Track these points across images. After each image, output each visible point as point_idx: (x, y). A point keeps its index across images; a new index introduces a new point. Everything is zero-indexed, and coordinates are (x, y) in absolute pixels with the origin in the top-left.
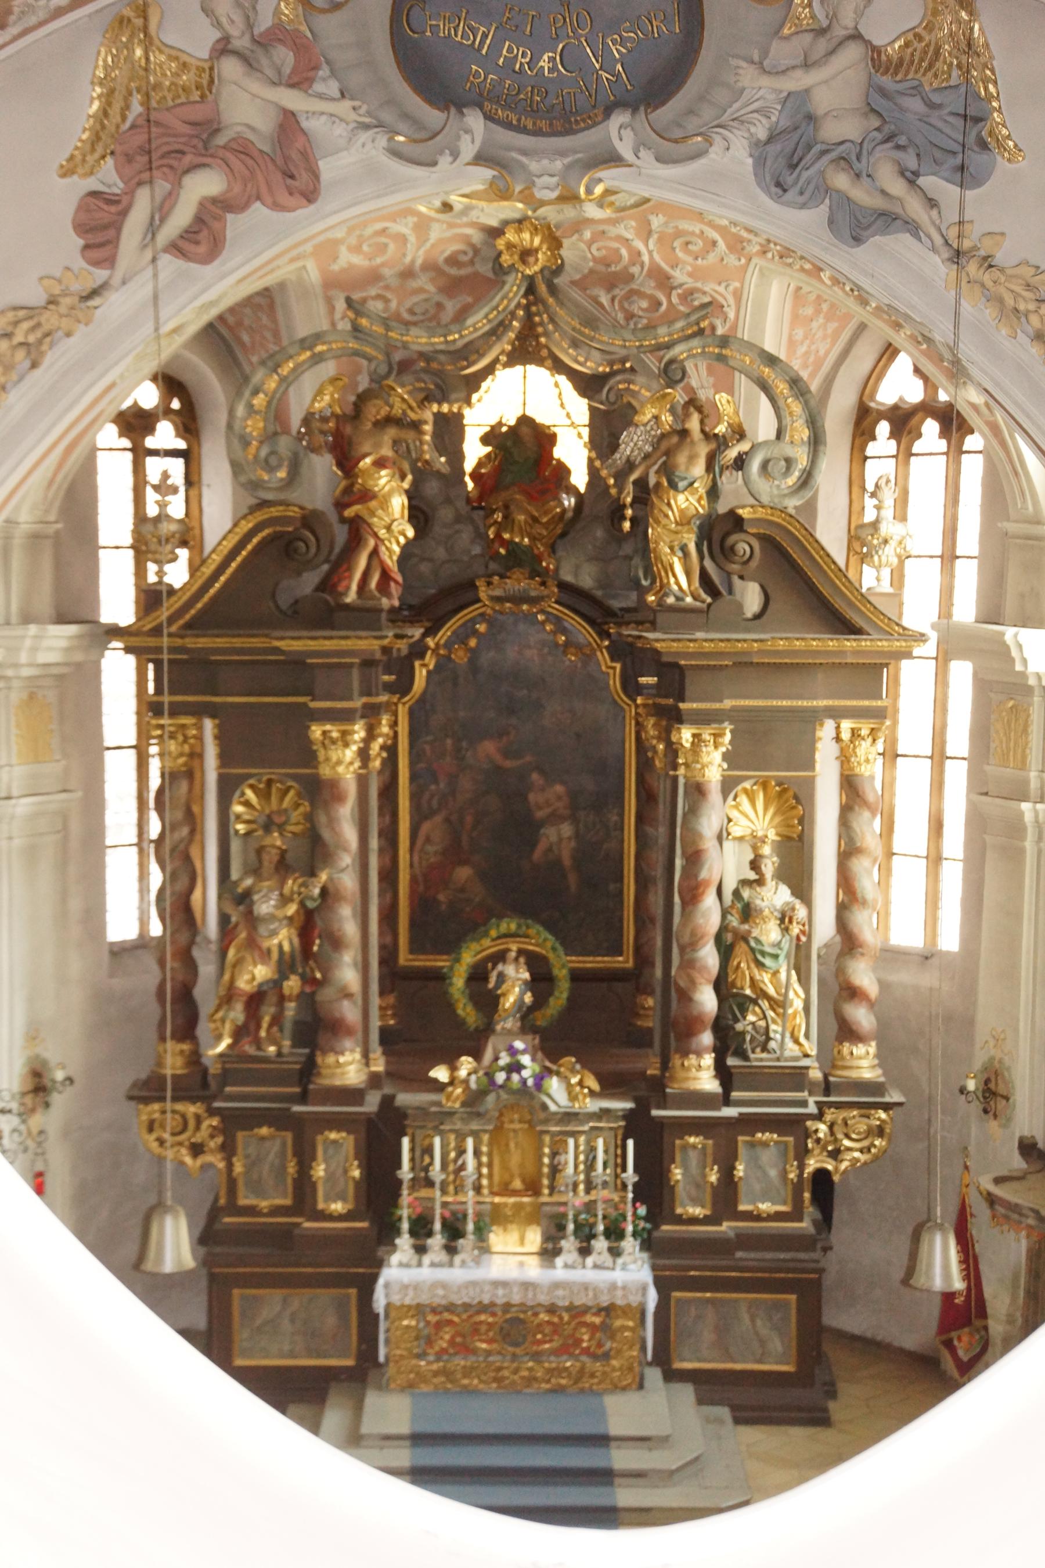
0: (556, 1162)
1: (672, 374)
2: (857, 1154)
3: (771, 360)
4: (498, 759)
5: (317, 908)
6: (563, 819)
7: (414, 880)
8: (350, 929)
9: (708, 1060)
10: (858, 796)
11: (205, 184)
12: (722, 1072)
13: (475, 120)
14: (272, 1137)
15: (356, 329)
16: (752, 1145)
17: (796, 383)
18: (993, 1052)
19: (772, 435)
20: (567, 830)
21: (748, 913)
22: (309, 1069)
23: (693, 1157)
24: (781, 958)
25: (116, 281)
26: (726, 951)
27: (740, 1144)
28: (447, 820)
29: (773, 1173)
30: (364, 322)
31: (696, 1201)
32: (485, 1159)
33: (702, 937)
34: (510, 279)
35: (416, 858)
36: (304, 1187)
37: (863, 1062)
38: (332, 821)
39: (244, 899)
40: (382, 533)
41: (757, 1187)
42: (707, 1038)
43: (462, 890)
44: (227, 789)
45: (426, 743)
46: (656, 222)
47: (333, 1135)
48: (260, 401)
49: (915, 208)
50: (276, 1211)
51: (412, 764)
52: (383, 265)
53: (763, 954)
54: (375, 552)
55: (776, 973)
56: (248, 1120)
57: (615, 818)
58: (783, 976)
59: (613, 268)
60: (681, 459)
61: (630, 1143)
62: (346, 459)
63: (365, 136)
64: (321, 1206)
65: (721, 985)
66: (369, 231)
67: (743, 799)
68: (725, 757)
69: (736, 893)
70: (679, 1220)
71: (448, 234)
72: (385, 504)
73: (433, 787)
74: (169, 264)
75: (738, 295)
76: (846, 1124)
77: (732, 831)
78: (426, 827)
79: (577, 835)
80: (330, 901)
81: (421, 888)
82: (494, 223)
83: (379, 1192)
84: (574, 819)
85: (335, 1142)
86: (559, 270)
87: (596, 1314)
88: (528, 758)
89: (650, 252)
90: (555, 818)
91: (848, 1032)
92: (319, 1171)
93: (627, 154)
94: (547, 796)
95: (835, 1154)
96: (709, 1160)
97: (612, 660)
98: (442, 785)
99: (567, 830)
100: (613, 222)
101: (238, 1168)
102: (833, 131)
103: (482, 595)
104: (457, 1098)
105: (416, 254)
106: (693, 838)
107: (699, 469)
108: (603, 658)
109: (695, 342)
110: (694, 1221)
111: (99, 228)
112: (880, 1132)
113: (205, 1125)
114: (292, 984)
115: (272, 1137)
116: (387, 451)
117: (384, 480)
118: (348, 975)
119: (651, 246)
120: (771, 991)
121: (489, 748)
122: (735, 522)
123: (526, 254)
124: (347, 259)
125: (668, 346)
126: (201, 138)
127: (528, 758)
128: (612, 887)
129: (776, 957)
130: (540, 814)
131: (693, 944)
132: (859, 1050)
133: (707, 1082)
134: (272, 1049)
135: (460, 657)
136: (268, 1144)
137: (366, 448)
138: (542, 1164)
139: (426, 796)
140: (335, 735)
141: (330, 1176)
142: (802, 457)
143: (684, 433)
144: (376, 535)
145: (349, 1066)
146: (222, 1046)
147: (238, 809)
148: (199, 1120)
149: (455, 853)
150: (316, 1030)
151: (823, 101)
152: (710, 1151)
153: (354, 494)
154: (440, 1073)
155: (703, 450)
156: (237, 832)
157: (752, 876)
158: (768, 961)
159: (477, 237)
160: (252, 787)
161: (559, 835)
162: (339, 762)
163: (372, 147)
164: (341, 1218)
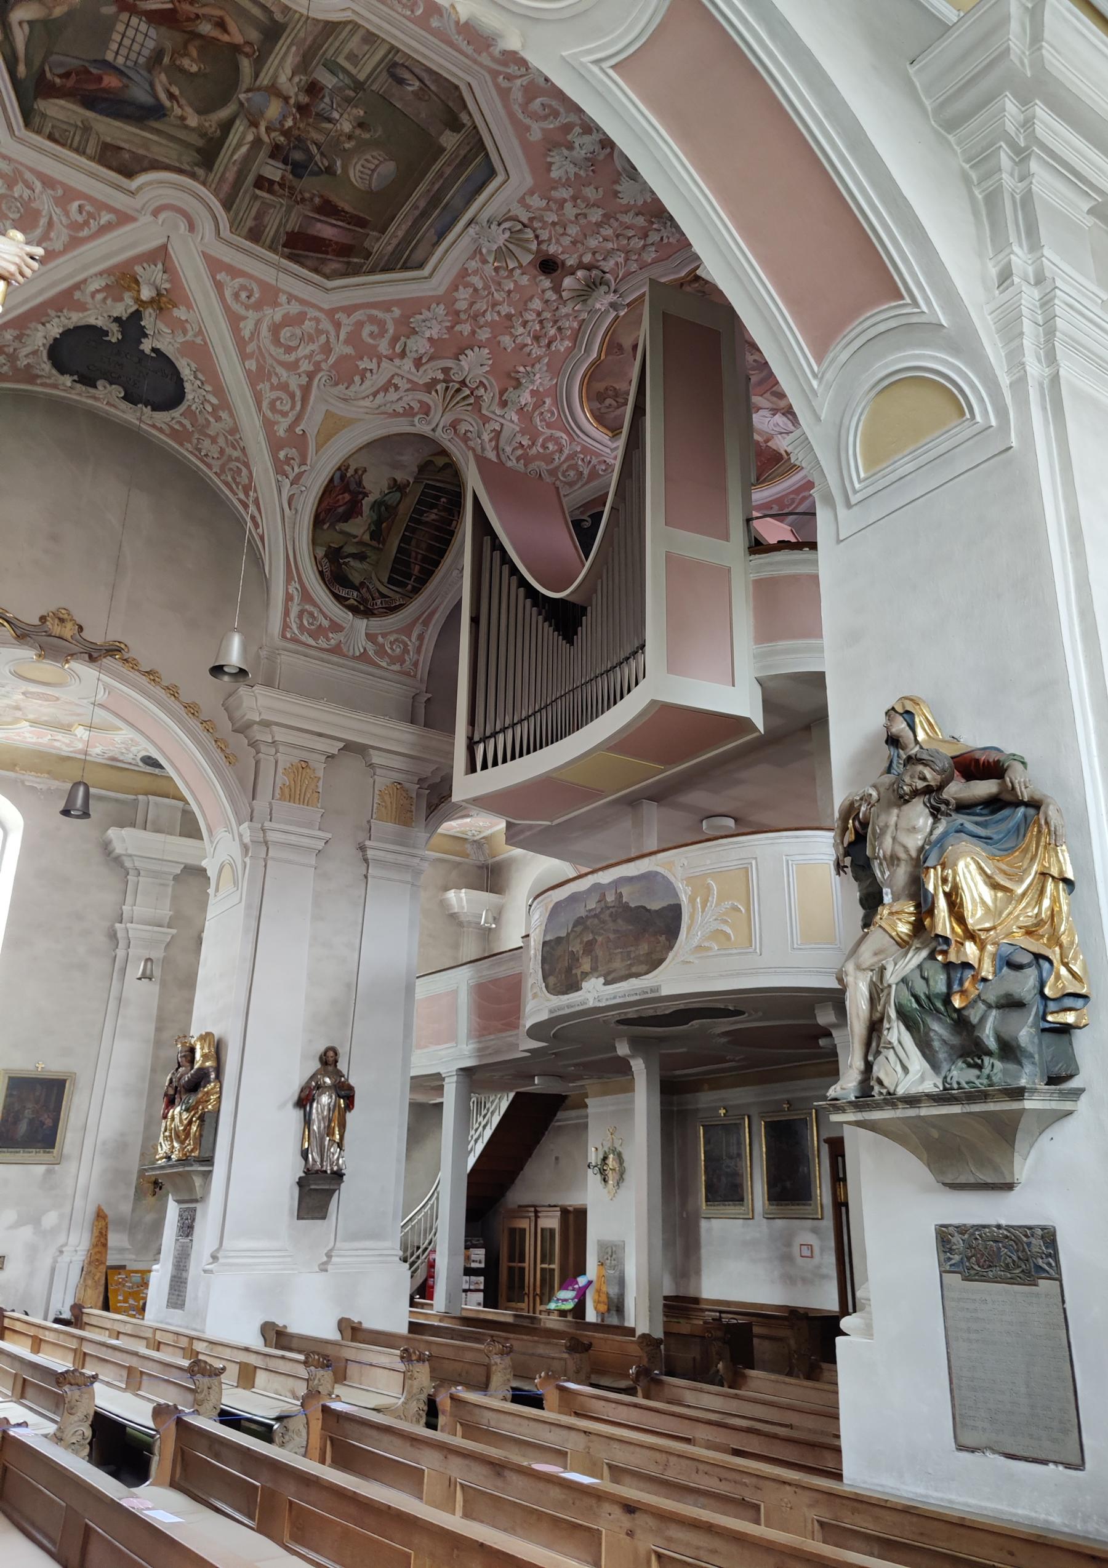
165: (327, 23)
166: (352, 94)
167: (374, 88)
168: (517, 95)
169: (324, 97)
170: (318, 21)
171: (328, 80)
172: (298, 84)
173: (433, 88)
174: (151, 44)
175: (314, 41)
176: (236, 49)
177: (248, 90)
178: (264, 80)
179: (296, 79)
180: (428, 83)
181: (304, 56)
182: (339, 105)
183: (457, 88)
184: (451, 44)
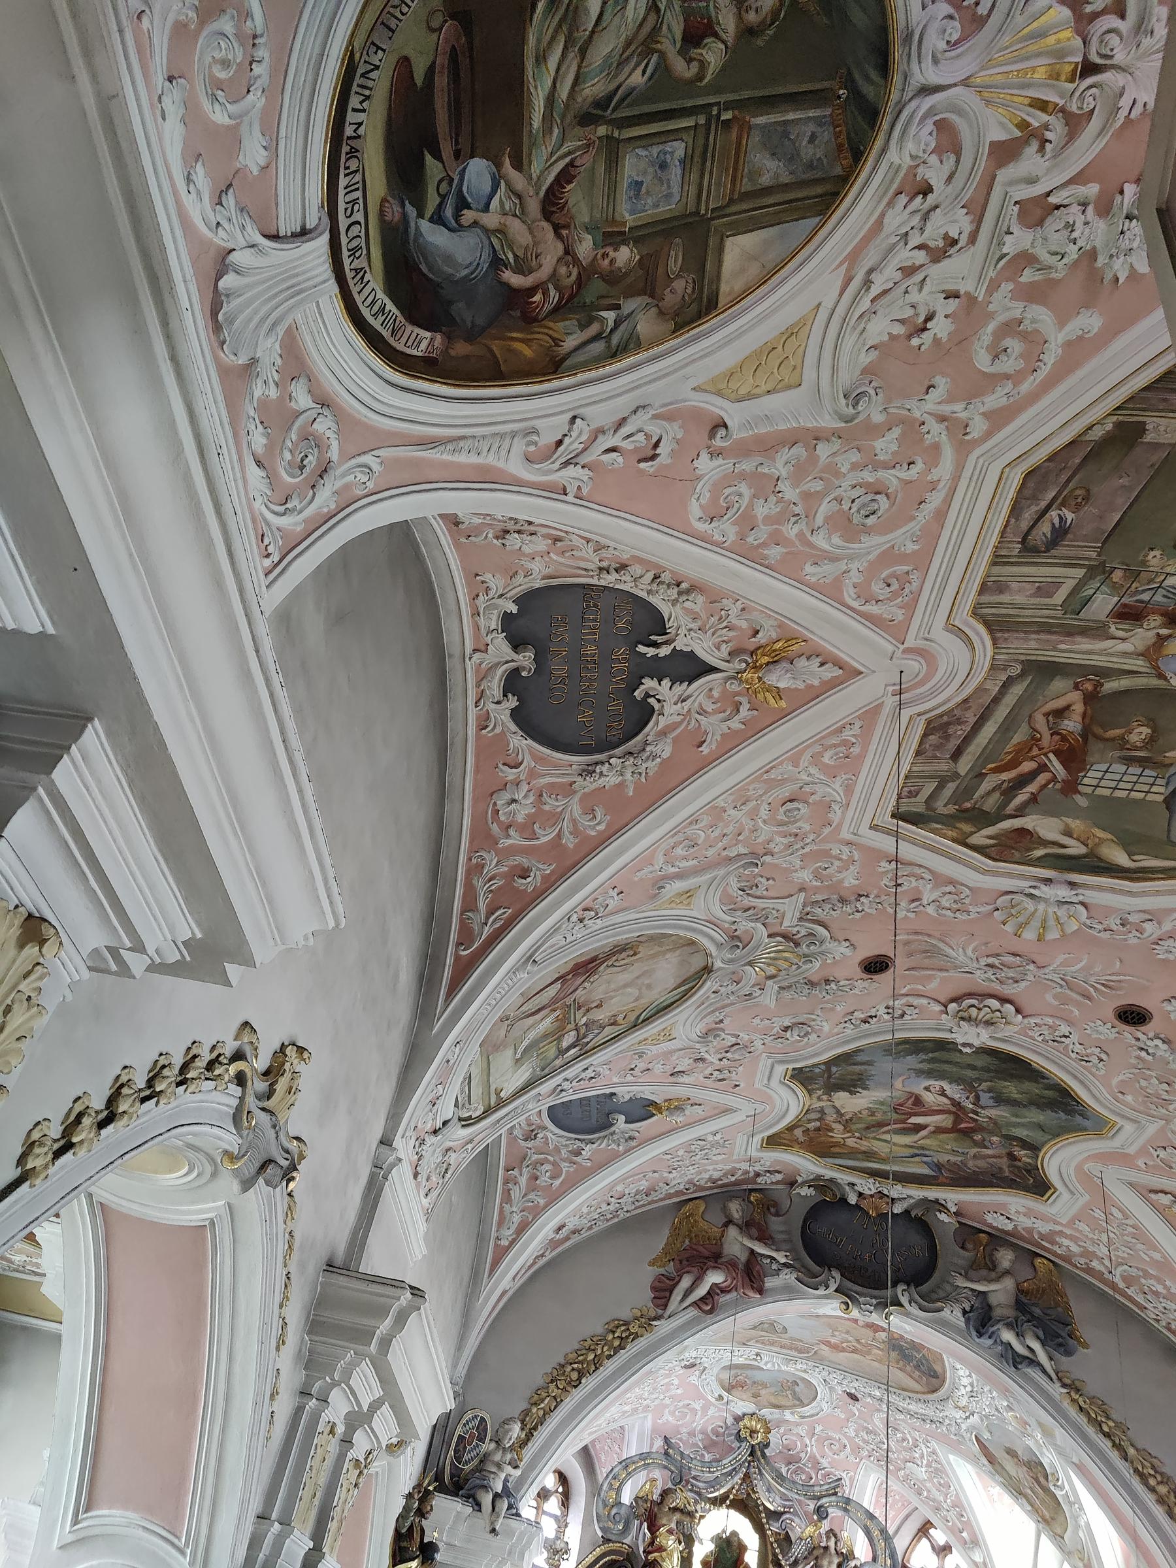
1: (822, 1513)
3: (872, 1517)
11: (715, 1277)
13: (836, 1274)
15: (666, 1453)
17: (883, 1530)
19: (870, 1559)
25: (666, 1315)
30: (671, 1451)
46: (818, 1429)
49: (1042, 1357)
52: (682, 1425)
62: (653, 1528)
63: (787, 1271)
66: (681, 1404)
72: (671, 1556)
74: (693, 1312)
75: (852, 1480)
82: (740, 1413)
86: (767, 1445)
89: (812, 1448)
93: (906, 1304)
100: (798, 1425)
102: (997, 1313)
105: (699, 1423)
109: (833, 1498)
111: (662, 1292)
116: (673, 1525)
123: (753, 1432)
124: (668, 1418)
125: (819, 1498)
126: (714, 1258)
137: (664, 1521)
143: (826, 1548)
151: (993, 1300)
153: (653, 1546)
155: (836, 1560)
159: (730, 1421)
163: (788, 1277)
165: (991, 631)
166: (1117, 576)
167: (1094, 555)
168: (995, 400)
169: (1142, 602)
170: (995, 641)
171: (1103, 604)
172: (1126, 631)
173: (1051, 495)
174: (1120, 768)
175: (1037, 632)
176: (1090, 698)
177: (1161, 676)
178: (1139, 664)
179: (1121, 634)
180: (1043, 504)
181: (1070, 634)
182: (1151, 581)
183: (1029, 475)
184: (941, 515)
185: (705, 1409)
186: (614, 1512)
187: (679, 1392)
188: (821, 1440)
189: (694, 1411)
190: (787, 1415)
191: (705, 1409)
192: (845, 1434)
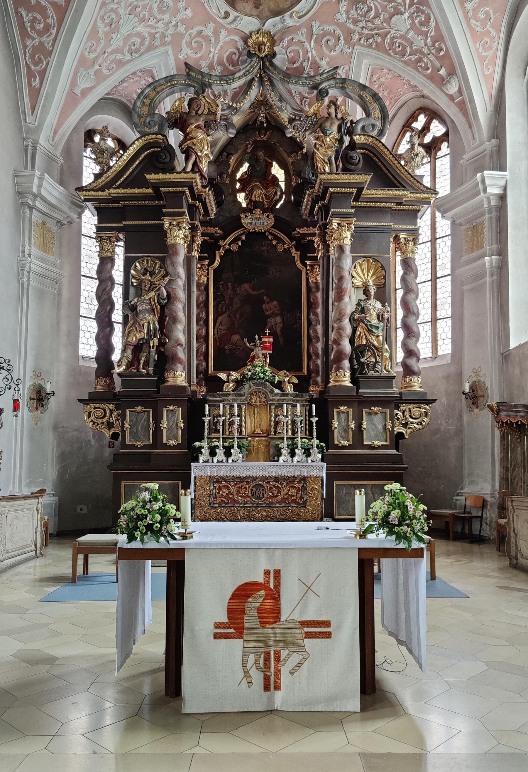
0: (277, 420)
1: (322, 94)
2: (416, 426)
3: (364, 87)
4: (250, 290)
5: (166, 303)
6: (277, 315)
7: (215, 340)
8: (181, 315)
9: (348, 374)
10: (409, 266)
12: (354, 380)
14: (144, 412)
16: (369, 414)
18: (474, 379)
20: (279, 319)
21: (363, 310)
22: (162, 380)
23: (343, 416)
24: (380, 329)
26: (354, 331)
27: (364, 412)
28: (229, 316)
29: (380, 427)
30: (193, 74)
31: (344, 438)
32: (243, 418)
33: (344, 315)
34: (255, 59)
35: (216, 330)
36: (158, 432)
37: (417, 384)
38: (173, 264)
39: (133, 309)
40: (200, 154)
41: (373, 433)
42: (346, 363)
43: (235, 345)
44: (128, 264)
45: (220, 284)
46: (315, 25)
47: (171, 408)
48: (147, 101)
50: (145, 447)
51: (215, 293)
53: (372, 326)
54: (195, 164)
55: (378, 337)
56: (132, 405)
57: (298, 315)
58: (381, 338)
59: (296, 65)
60: (328, 124)
61: (314, 406)
64: (165, 441)
65: (352, 341)
66: (194, 31)
67: (358, 267)
68: (352, 235)
69: (358, 304)
70: (337, 447)
71: (228, 39)
73: (223, 302)
76: (410, 411)
77: (355, 274)
78: (220, 319)
79: (283, 322)
80: (172, 301)
81: (218, 344)
83: (194, 430)
84: (282, 316)
85: (172, 411)
86: (275, 55)
87: (298, 482)
88: (262, 291)
90: (274, 315)
91: (408, 371)
92: (164, 424)
94: (271, 307)
95: (405, 425)
96: (351, 417)
97: (296, 251)
98: (227, 302)
99: (279, 319)
100: (296, 29)
101: (127, 425)
103: (244, 222)
104: (231, 388)
106: (340, 269)
107: (335, 128)
108: (293, 251)
109: (332, 82)
110: (344, 447)
112: (426, 415)
113: (115, 414)
114: (154, 342)
115: (144, 412)
117: (200, 135)
118: (179, 333)
119: (313, 46)
120: (375, 343)
121: (246, 286)
122: (353, 145)
123: (260, 45)
124: (187, 54)
127: (262, 291)
128: (298, 343)
129: (377, 328)
130: (267, 313)
131: (339, 319)
132: (415, 379)
133: (347, 382)
134: (144, 371)
135: (234, 248)
136: (141, 414)
138: (271, 421)
139: (220, 306)
140: (175, 223)
141: (169, 429)
142: (379, 124)
144: (196, 154)
145: (179, 377)
146: (121, 369)
147: (133, 272)
148: (111, 411)
149: (231, 330)
150: (165, 360)
152: (351, 413)
154: (223, 376)
155: (337, 123)
156: (132, 283)
157: (364, 297)
158: (374, 330)
159: (240, 44)
160: (139, 262)
161: (275, 322)
162: (177, 236)
164: (174, 447)
185: (216, 33)
186: (148, 120)
187: (189, 13)
188: (318, 41)
189: (207, 39)
190: (289, 20)
191: (216, 33)
192: (338, 24)
